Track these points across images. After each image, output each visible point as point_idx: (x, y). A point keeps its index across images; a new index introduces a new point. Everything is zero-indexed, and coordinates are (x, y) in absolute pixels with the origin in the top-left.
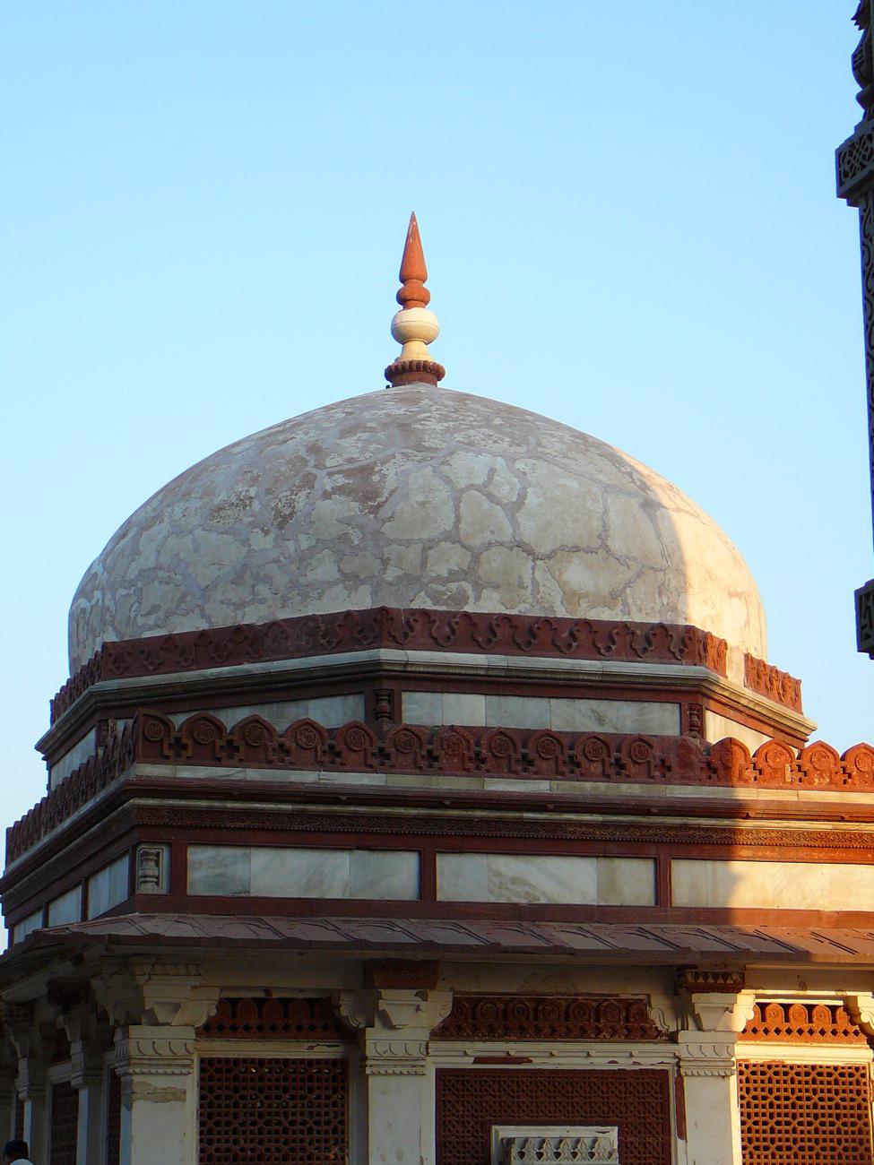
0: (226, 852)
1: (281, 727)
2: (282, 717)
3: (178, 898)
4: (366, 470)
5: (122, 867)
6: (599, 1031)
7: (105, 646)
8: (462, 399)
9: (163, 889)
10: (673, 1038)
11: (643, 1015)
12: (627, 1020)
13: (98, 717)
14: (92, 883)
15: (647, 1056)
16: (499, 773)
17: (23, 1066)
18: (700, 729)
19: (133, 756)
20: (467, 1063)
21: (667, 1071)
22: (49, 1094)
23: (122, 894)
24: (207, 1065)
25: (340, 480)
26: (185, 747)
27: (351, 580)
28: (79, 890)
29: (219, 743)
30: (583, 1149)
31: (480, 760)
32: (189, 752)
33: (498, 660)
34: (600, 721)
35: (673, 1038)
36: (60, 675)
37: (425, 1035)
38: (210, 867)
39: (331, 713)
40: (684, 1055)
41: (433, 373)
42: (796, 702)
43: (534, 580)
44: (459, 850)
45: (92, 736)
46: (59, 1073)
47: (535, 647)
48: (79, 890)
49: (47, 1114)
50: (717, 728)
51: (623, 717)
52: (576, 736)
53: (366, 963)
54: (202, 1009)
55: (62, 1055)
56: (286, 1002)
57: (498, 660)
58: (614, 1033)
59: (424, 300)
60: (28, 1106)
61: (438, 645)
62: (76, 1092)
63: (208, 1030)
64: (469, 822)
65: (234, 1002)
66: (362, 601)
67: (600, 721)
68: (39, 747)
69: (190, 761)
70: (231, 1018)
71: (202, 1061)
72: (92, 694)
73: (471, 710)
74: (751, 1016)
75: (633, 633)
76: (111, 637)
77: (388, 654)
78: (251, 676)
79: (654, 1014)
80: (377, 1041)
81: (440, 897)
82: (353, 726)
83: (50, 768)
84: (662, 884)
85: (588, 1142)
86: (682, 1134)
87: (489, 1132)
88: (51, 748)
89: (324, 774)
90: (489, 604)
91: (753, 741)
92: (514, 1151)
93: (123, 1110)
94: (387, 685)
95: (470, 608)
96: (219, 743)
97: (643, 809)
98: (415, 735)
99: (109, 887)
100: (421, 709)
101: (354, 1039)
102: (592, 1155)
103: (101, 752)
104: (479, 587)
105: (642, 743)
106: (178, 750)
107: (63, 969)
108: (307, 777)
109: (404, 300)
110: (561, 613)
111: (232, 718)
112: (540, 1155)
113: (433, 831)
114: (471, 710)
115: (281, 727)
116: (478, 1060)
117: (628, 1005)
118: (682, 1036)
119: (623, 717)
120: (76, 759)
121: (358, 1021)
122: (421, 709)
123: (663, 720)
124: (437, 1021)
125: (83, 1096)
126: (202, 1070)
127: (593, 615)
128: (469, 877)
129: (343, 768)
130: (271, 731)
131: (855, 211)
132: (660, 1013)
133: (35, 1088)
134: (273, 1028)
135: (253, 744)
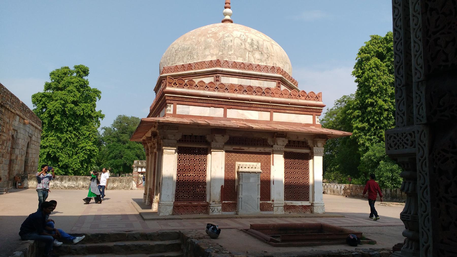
2: (197, 81)
4: (216, 33)
6: (258, 144)
10: (272, 146)
11: (266, 142)
22: (154, 154)
25: (211, 35)
26: (176, 84)
27: (212, 55)
29: (184, 84)
32: (178, 85)
37: (224, 144)
39: (207, 80)
43: (248, 56)
46: (155, 150)
51: (265, 84)
54: (179, 137)
56: (196, 136)
58: (261, 145)
63: (179, 141)
65: (185, 136)
66: (214, 58)
67: (260, 84)
72: (161, 77)
79: (269, 142)
80: (213, 144)
81: (227, 117)
82: (211, 83)
84: (271, 116)
86: (273, 165)
90: (240, 60)
95: (236, 61)
100: (225, 80)
108: (202, 92)
110: (253, 63)
114: (235, 81)
116: (233, 149)
117: (264, 139)
119: (265, 84)
121: (209, 141)
130: (194, 82)
132: (270, 141)
134: (193, 141)
135: (191, 85)
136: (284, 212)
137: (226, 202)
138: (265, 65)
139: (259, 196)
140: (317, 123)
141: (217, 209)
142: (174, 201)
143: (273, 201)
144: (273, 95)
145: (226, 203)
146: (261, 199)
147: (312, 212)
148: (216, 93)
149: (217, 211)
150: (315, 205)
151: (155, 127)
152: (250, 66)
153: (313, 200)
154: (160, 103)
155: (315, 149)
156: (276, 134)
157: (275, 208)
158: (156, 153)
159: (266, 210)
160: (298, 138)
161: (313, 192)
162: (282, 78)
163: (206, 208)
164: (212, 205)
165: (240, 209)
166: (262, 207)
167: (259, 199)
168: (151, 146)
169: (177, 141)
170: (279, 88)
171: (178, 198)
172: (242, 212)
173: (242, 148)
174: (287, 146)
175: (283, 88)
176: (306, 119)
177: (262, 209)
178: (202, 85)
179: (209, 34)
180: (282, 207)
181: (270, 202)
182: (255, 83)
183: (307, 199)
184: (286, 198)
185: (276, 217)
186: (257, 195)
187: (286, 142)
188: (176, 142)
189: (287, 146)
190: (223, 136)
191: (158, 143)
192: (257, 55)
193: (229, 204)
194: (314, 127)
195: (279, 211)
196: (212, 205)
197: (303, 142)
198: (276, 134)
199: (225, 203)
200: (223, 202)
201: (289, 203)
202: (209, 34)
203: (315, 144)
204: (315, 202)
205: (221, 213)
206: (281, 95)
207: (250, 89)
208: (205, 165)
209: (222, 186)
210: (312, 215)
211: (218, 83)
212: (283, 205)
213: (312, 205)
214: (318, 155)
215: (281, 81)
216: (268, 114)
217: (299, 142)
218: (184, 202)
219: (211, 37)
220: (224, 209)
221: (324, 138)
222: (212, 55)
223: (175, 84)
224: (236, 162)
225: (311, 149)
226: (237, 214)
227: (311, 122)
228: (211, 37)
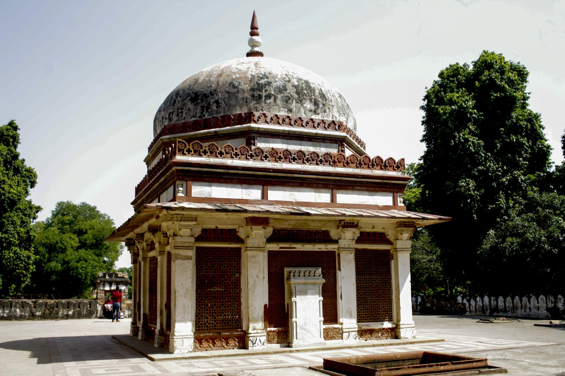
7: (165, 126)
12: (324, 236)
13: (163, 147)
14: (161, 196)
15: (331, 247)
20: (278, 249)
21: (335, 252)
22: (148, 260)
24: (198, 249)
30: (312, 274)
31: (280, 158)
35: (336, 242)
36: (151, 138)
40: (341, 246)
42: (364, 148)
45: (161, 153)
46: (152, 254)
50: (348, 153)
53: (246, 218)
54: (198, 232)
59: (257, 35)
60: (142, 263)
62: (157, 259)
63: (198, 239)
68: (145, 161)
71: (197, 248)
74: (359, 235)
75: (325, 123)
76: (166, 123)
77: (253, 125)
78: (210, 132)
80: (250, 243)
83: (148, 167)
85: (313, 272)
86: (340, 270)
87: (284, 270)
88: (148, 161)
89: (234, 161)
90: (283, 113)
92: (292, 275)
93: (172, 262)
94: (253, 135)
96: (201, 150)
97: (329, 174)
102: (314, 276)
103: (164, 156)
107: (153, 221)
109: (252, 34)
112: (299, 276)
113: (266, 180)
116: (280, 248)
117: (324, 232)
118: (340, 241)
125: (159, 258)
126: (197, 251)
133: (144, 259)
138: (320, 118)
139: (322, 319)
140: (400, 204)
142: (194, 331)
143: (342, 324)
144: (334, 164)
145: (273, 332)
146: (325, 322)
149: (260, 344)
151: (158, 217)
152: (299, 121)
153: (399, 320)
154: (162, 179)
155: (399, 244)
156: (343, 223)
157: (345, 335)
158: (154, 260)
159: (332, 338)
160: (373, 227)
161: (398, 308)
162: (346, 137)
164: (251, 335)
165: (295, 339)
167: (322, 323)
168: (143, 249)
169: (195, 238)
170: (342, 153)
171: (199, 327)
173: (293, 246)
174: (358, 241)
175: (348, 153)
180: (354, 333)
181: (340, 326)
187: (357, 233)
188: (193, 240)
189: (358, 241)
190: (265, 228)
191: (160, 243)
192: (309, 105)
194: (396, 211)
196: (251, 335)
198: (343, 223)
199: (270, 331)
200: (269, 329)
201: (366, 326)
204: (401, 323)
205: (265, 347)
206: (347, 164)
207: (301, 157)
208: (237, 275)
209: (265, 306)
212: (357, 329)
214: (403, 250)
215: (340, 142)
217: (375, 233)
218: (209, 333)
221: (412, 227)
223: (189, 151)
224: (285, 269)
226: (289, 347)
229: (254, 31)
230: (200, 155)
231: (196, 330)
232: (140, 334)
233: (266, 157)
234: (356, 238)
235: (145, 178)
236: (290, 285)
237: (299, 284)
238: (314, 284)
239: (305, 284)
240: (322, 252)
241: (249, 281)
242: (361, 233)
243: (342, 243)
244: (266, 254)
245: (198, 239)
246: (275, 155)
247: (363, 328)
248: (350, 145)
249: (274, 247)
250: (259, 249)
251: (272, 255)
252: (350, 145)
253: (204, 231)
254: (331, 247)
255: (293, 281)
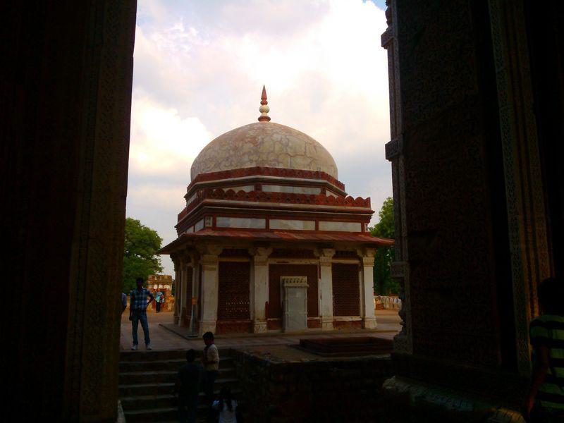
0: (225, 218)
1: (236, 192)
2: (237, 190)
3: (214, 228)
4: (255, 138)
5: (202, 221)
8: (275, 124)
9: (211, 226)
10: (319, 258)
15: (314, 262)
16: (282, 202)
17: (181, 263)
18: (325, 194)
19: (204, 197)
23: (202, 227)
25: (249, 140)
27: (251, 161)
28: (193, 227)
33: (283, 178)
34: (304, 191)
37: (267, 257)
38: (222, 221)
39: (248, 189)
41: (269, 119)
42: (344, 189)
44: (274, 218)
46: (189, 265)
47: (289, 175)
48: (193, 227)
49: (186, 273)
52: (299, 194)
54: (220, 251)
55: (190, 261)
57: (283, 178)
61: (270, 175)
63: (221, 256)
64: (276, 212)
66: (254, 165)
67: (304, 191)
69: (217, 199)
70: (226, 253)
73: (277, 189)
80: (256, 259)
84: (317, 226)
86: (320, 278)
88: (187, 197)
91: (336, 196)
95: (277, 167)
97: (313, 210)
98: (265, 194)
99: (199, 226)
101: (251, 257)
104: (279, 163)
105: (313, 196)
106: (215, 196)
108: (242, 202)
109: (262, 103)
111: (226, 190)
113: (269, 214)
114: (277, 189)
115: (236, 192)
120: (192, 199)
121: (252, 254)
122: (267, 189)
123: (317, 191)
124: (269, 254)
125: (194, 269)
127: (303, 169)
128: (275, 224)
129: (250, 200)
131: (386, 51)
132: (316, 253)
135: (231, 195)
136: (333, 329)
137: (271, 319)
139: (306, 313)
141: (261, 327)
143: (321, 317)
147: (363, 327)
148: (257, 203)
150: (367, 320)
152: (292, 173)
153: (364, 315)
155: (365, 260)
157: (323, 325)
161: (364, 306)
163: (251, 326)
166: (310, 324)
172: (288, 329)
174: (334, 257)
175: (328, 194)
176: (354, 227)
177: (309, 327)
178: (243, 195)
179: (247, 138)
182: (298, 190)
183: (357, 314)
184: (335, 314)
185: (325, 333)
186: (303, 312)
187: (333, 253)
193: (275, 321)
194: (363, 236)
195: (328, 326)
197: (352, 252)
202: (247, 138)
203: (364, 253)
209: (267, 302)
210: (363, 330)
211: (259, 192)
213: (363, 320)
216: (313, 223)
219: (250, 142)
220: (270, 326)
222: (251, 161)
225: (360, 259)
227: (360, 231)
228: (250, 142)
229: (264, 101)
230: (223, 199)
231: (218, 319)
232: (180, 322)
233: (269, 199)
234: (332, 255)
235: (184, 210)
236: (284, 288)
237: (290, 287)
238: (301, 287)
239: (295, 287)
240: (308, 265)
241: (256, 284)
242: (337, 252)
243: (322, 259)
244: (267, 267)
245: (221, 256)
246: (274, 197)
247: (337, 320)
248: (331, 189)
249: (274, 261)
250: (263, 263)
251: (271, 267)
252: (331, 189)
253: (225, 250)
254: (314, 262)
255: (286, 285)
